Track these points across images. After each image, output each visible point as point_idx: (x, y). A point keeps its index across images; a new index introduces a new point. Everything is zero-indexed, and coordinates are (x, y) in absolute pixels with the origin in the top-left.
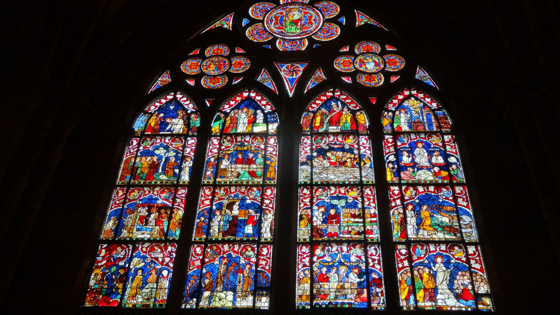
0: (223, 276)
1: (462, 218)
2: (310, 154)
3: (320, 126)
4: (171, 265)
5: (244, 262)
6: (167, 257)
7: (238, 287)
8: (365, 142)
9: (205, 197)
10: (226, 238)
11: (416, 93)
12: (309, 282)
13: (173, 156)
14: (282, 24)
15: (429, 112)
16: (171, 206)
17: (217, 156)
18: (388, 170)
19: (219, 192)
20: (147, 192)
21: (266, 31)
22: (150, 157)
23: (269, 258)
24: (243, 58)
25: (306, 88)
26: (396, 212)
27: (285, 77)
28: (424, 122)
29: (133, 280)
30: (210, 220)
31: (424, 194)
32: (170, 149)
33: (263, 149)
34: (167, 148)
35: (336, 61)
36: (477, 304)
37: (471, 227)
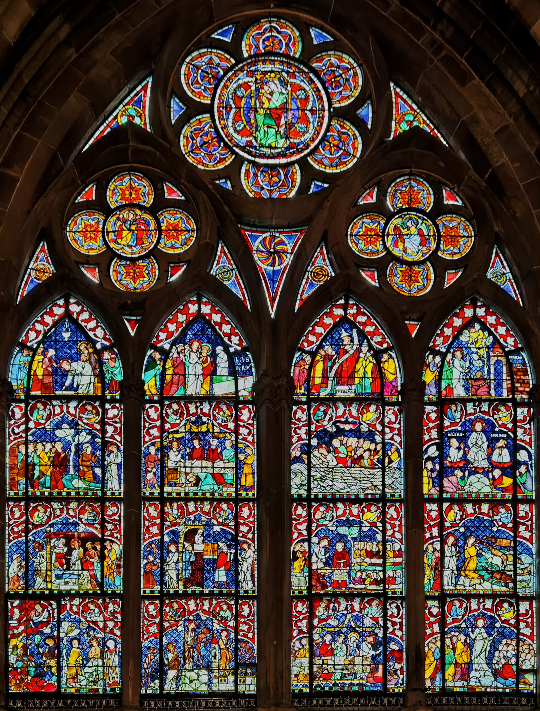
0: (192, 647)
1: (520, 559)
2: (307, 442)
3: (322, 383)
4: (118, 633)
5: (218, 628)
6: (110, 620)
7: (213, 664)
8: (393, 419)
9: (150, 521)
10: (189, 591)
11: (484, 314)
12: (307, 655)
13: (88, 442)
14: (248, 122)
15: (500, 358)
16: (100, 536)
17: (159, 444)
18: (425, 472)
19: (170, 511)
20: (58, 512)
21: (220, 139)
22: (49, 444)
23: (253, 621)
24: (180, 213)
25: (299, 298)
26: (431, 549)
27: (261, 268)
28: (490, 379)
29: (68, 655)
30: (163, 561)
31: (473, 518)
32: (80, 427)
33: (232, 431)
34: (74, 425)
35: (352, 229)
36: (517, 683)
37: (529, 573)
